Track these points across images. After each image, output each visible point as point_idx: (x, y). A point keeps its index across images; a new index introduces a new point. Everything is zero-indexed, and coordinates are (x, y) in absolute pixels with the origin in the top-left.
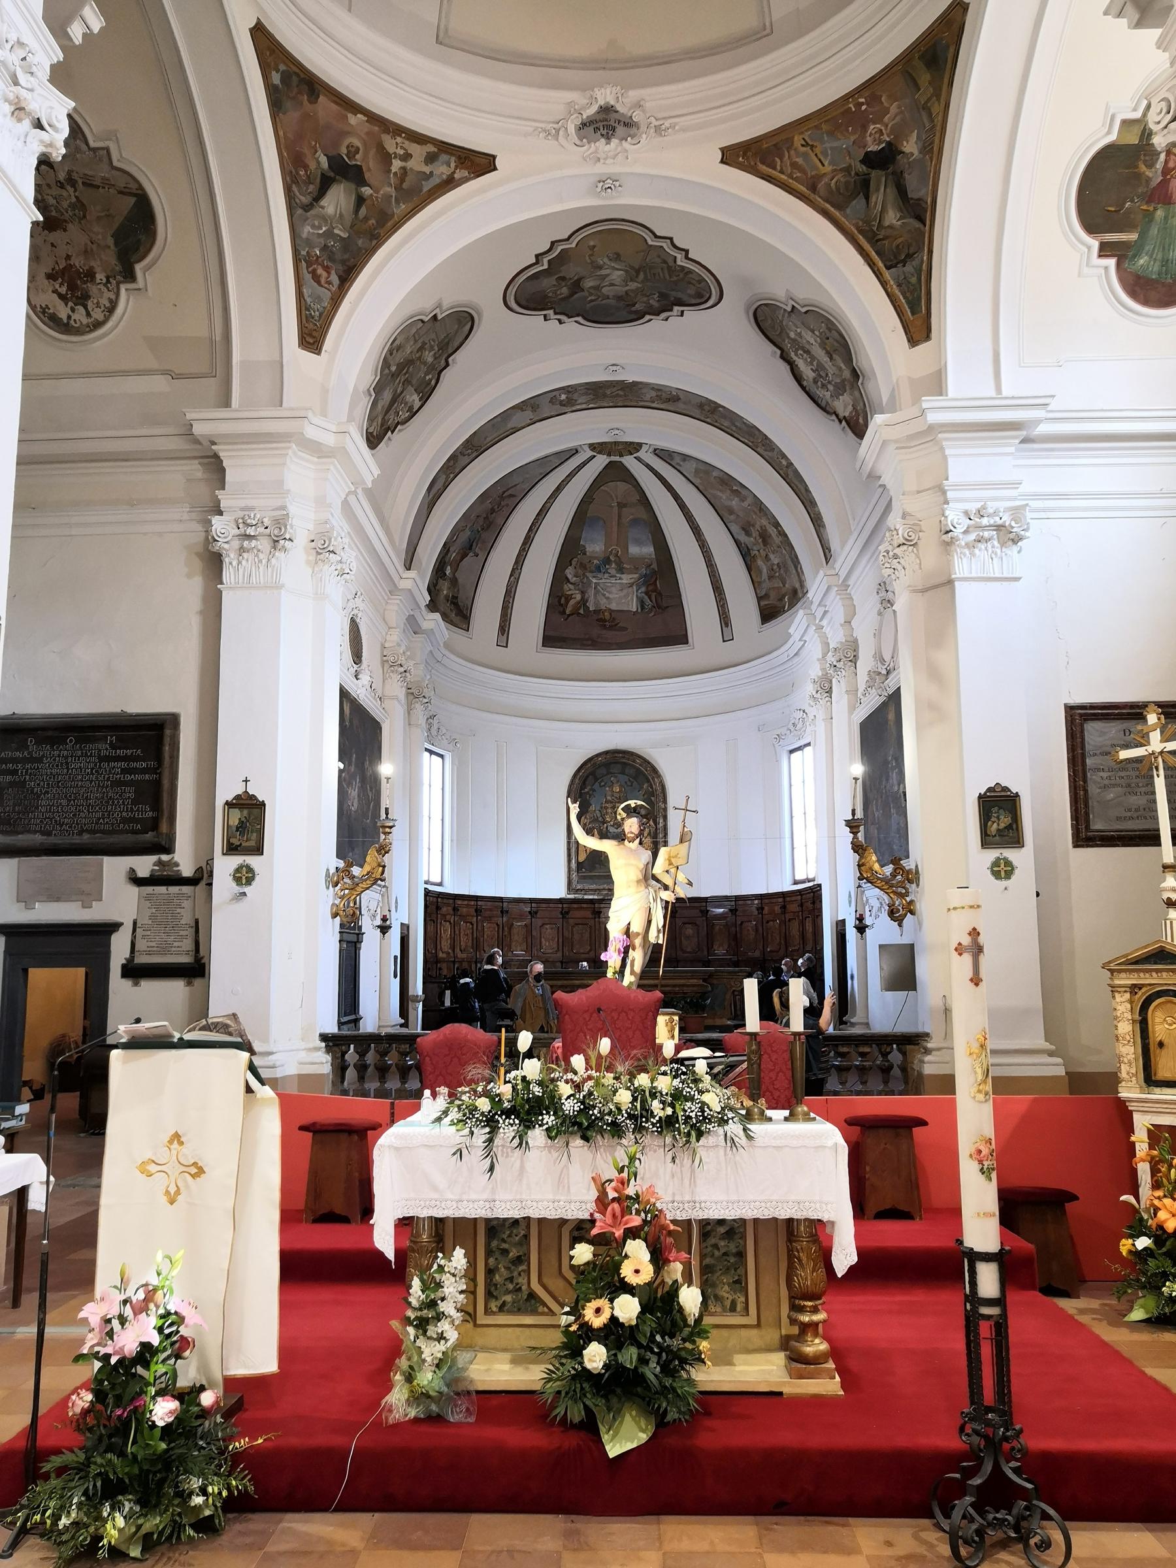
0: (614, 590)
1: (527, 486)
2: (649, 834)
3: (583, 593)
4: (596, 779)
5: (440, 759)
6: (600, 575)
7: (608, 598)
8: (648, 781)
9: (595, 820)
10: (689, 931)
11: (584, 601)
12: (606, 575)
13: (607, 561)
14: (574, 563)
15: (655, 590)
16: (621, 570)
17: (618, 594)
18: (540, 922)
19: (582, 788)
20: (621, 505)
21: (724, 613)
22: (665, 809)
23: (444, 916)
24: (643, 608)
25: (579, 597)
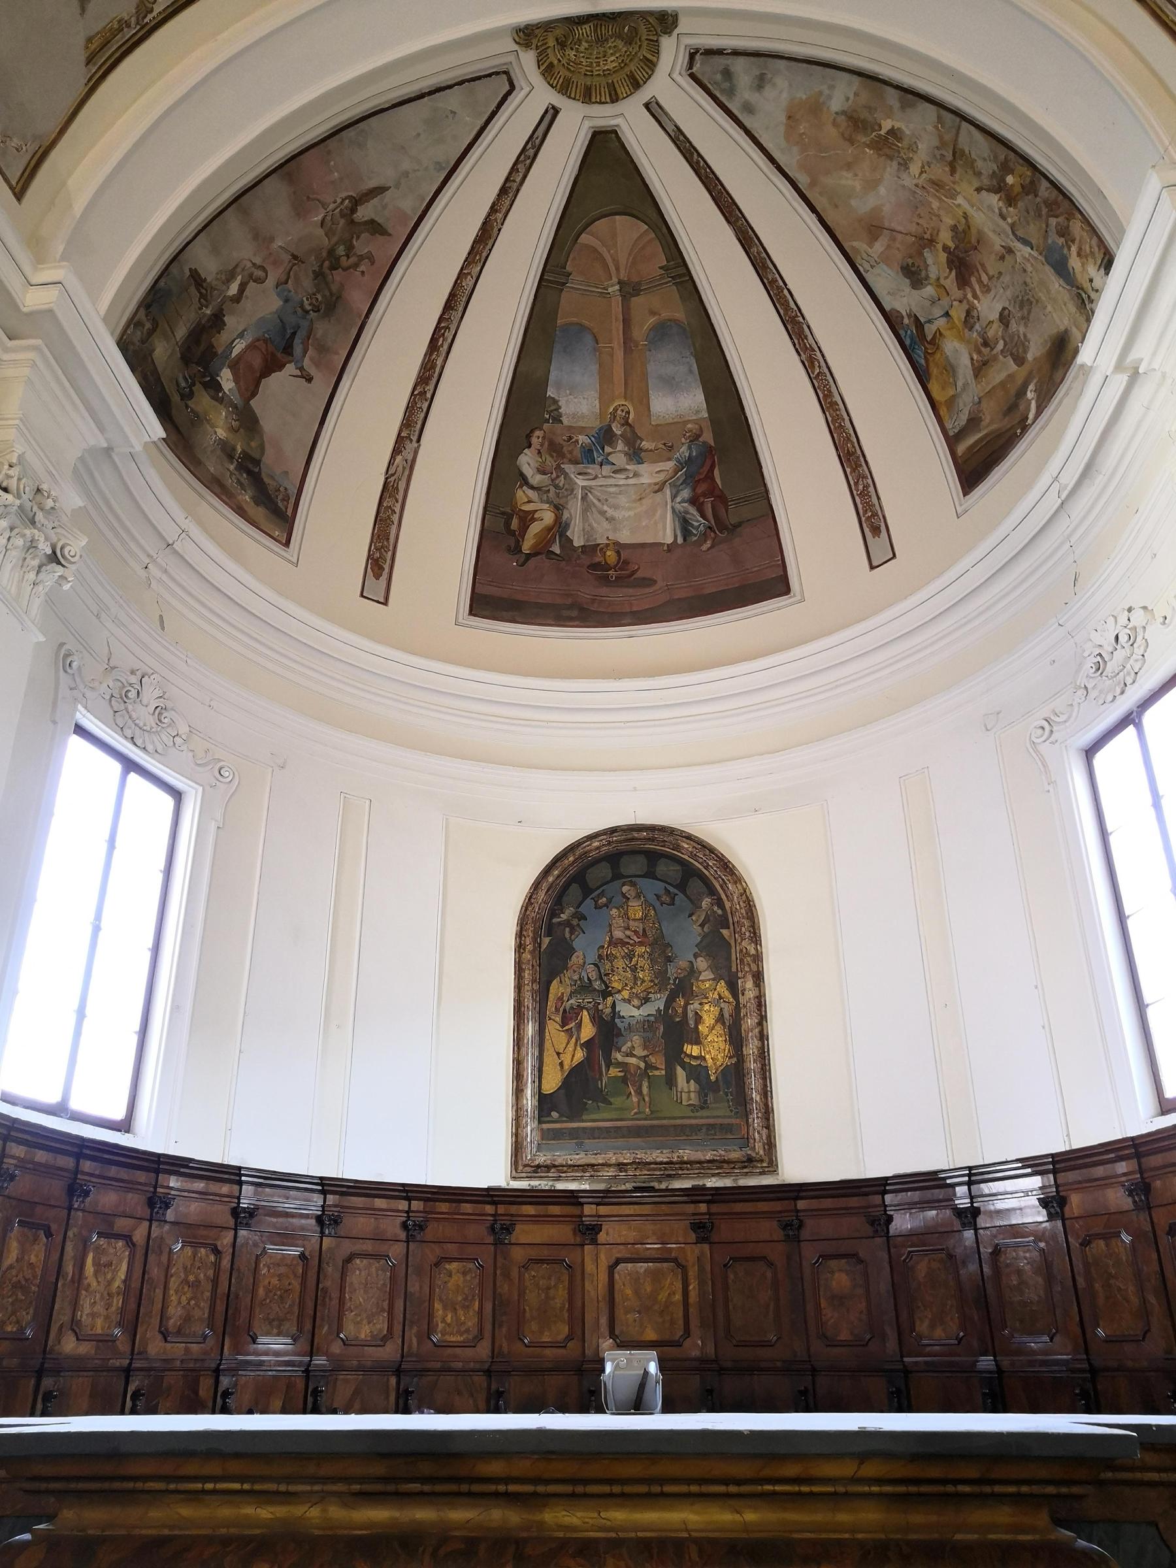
0: (623, 500)
1: (410, 205)
2: (720, 1019)
3: (558, 509)
4: (587, 891)
5: (169, 802)
6: (593, 469)
7: (610, 520)
8: (712, 891)
9: (584, 988)
10: (840, 1278)
11: (560, 528)
12: (606, 470)
13: (606, 436)
14: (534, 440)
15: (712, 491)
16: (636, 455)
17: (632, 506)
18: (431, 1253)
19: (553, 914)
20: (630, 290)
21: (868, 506)
22: (758, 958)
23: (107, 1218)
24: (686, 533)
25: (548, 517)
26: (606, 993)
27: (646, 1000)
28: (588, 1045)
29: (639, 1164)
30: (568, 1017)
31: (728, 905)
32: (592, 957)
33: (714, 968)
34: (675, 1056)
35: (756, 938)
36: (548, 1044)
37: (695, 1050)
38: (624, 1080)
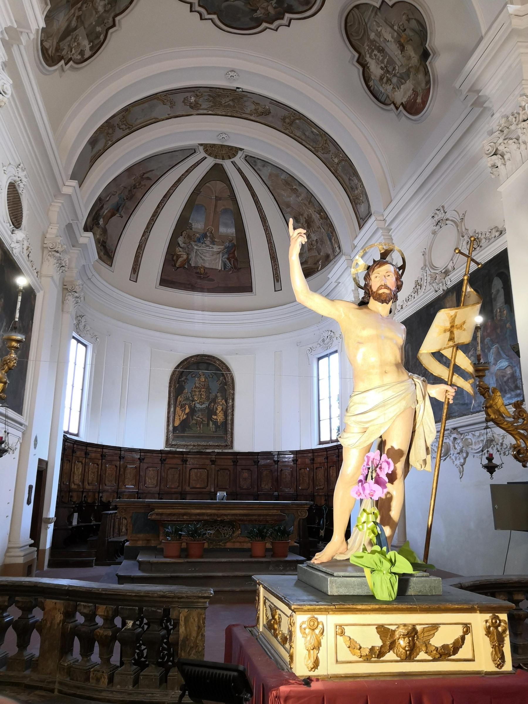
0: (207, 255)
1: (159, 174)
2: (222, 409)
3: (188, 254)
5: (84, 348)
6: (199, 244)
7: (203, 260)
9: (187, 399)
10: (246, 474)
11: (188, 260)
12: (204, 245)
13: (205, 236)
14: (183, 234)
15: (234, 257)
16: (213, 242)
17: (210, 257)
18: (145, 466)
19: (179, 378)
20: (218, 199)
21: (277, 273)
22: (233, 394)
23: (78, 458)
24: (225, 268)
25: (185, 257)
26: (193, 401)
27: (204, 403)
28: (187, 414)
29: (198, 445)
30: (183, 407)
31: (227, 379)
32: (190, 391)
33: (221, 396)
34: (210, 418)
35: (233, 389)
36: (176, 413)
37: (215, 417)
38: (196, 424)
